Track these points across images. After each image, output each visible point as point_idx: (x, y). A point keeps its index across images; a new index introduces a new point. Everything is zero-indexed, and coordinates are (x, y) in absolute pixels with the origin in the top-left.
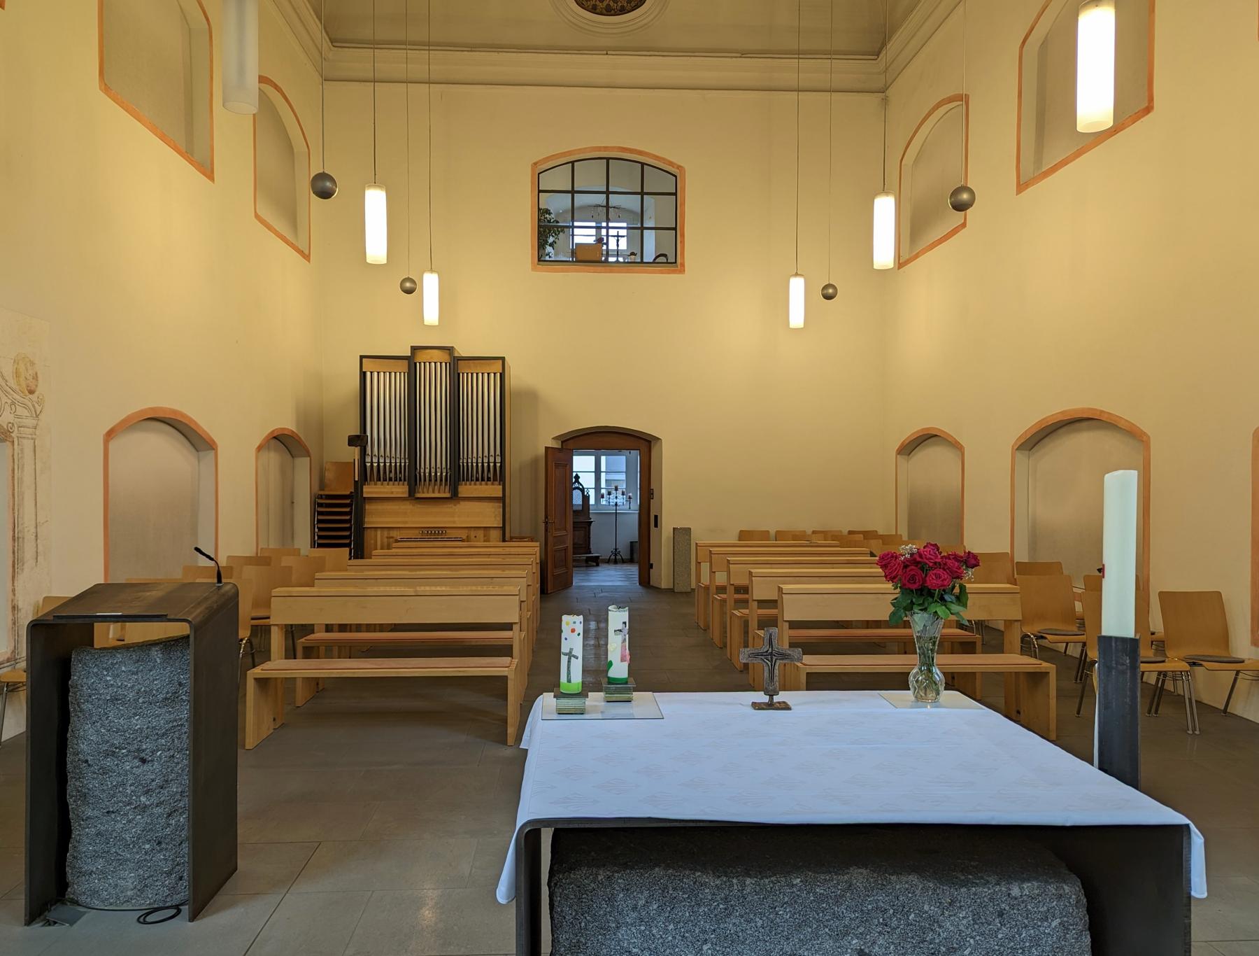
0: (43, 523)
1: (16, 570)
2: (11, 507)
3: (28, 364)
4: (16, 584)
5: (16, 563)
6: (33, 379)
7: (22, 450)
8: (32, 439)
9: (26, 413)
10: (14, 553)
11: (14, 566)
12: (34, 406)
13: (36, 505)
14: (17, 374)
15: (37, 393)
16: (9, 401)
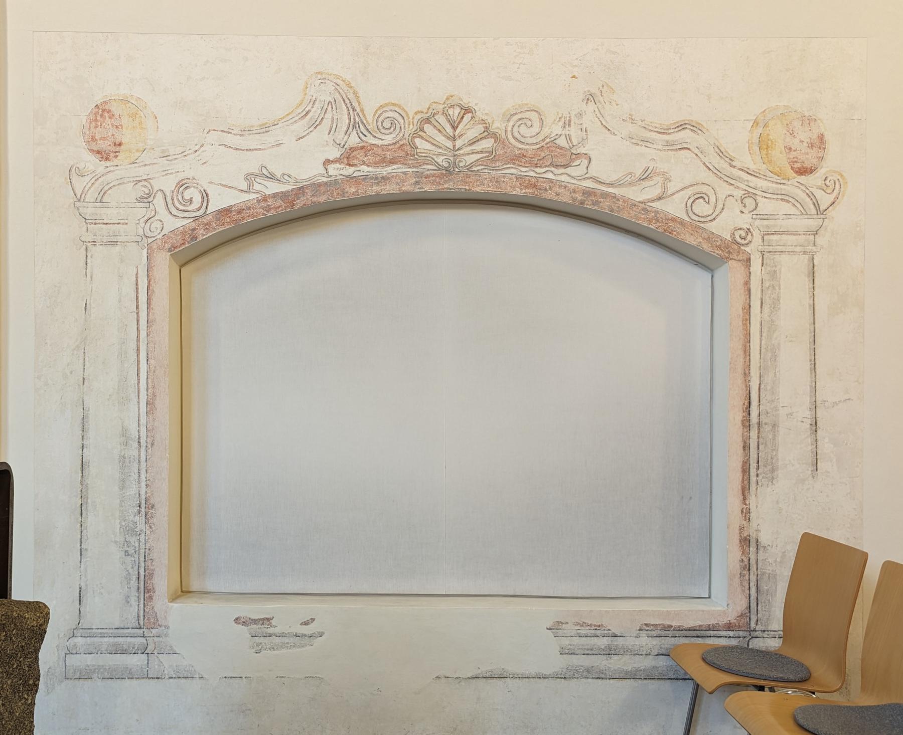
0: (835, 404)
1: (753, 479)
2: (740, 370)
3: (797, 124)
4: (752, 500)
5: (753, 465)
6: (812, 146)
7: (774, 275)
8: (805, 253)
9: (786, 208)
10: (746, 447)
11: (746, 470)
12: (810, 195)
13: (814, 368)
14: (764, 144)
15: (821, 172)
16: (739, 193)
